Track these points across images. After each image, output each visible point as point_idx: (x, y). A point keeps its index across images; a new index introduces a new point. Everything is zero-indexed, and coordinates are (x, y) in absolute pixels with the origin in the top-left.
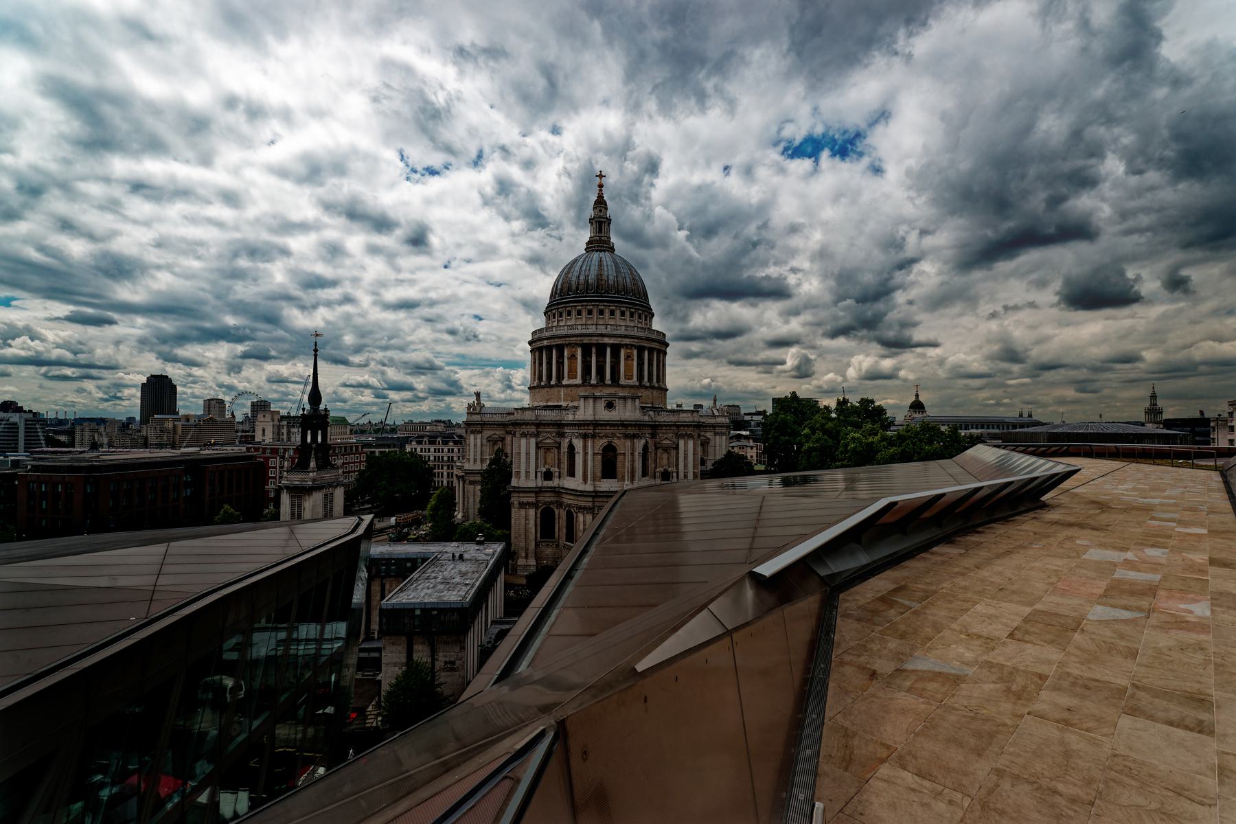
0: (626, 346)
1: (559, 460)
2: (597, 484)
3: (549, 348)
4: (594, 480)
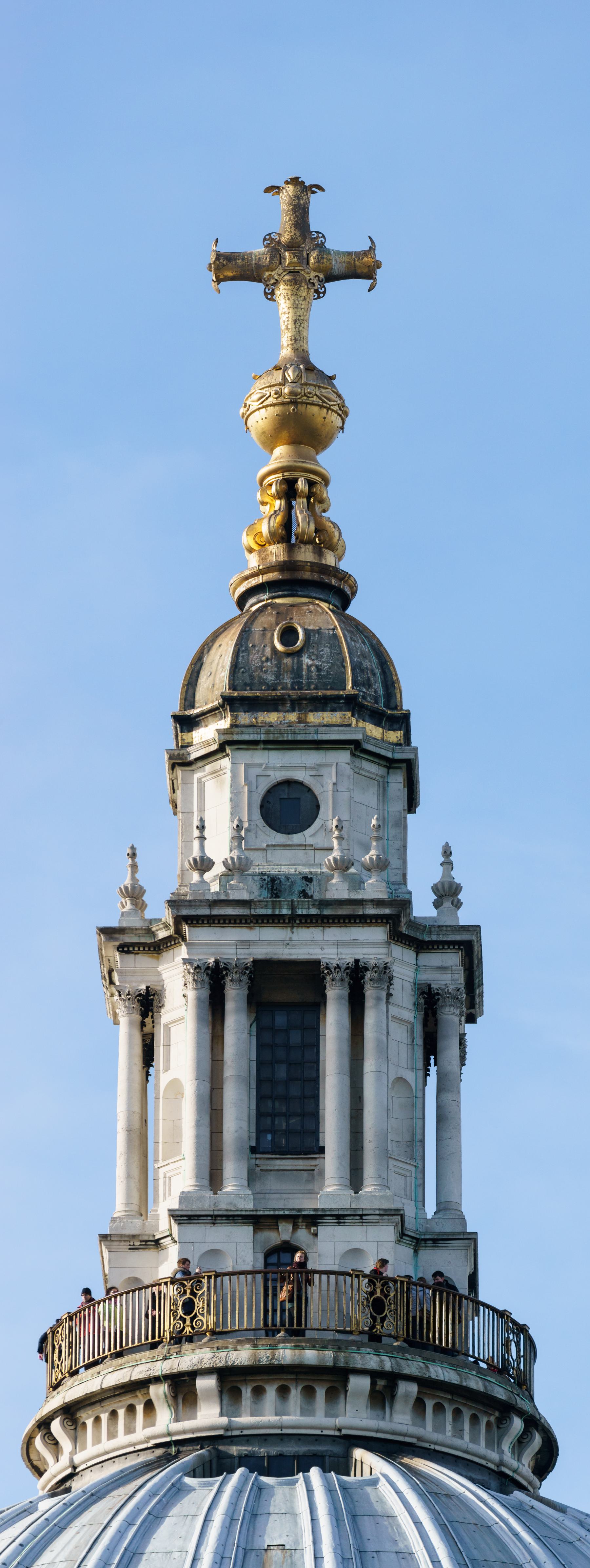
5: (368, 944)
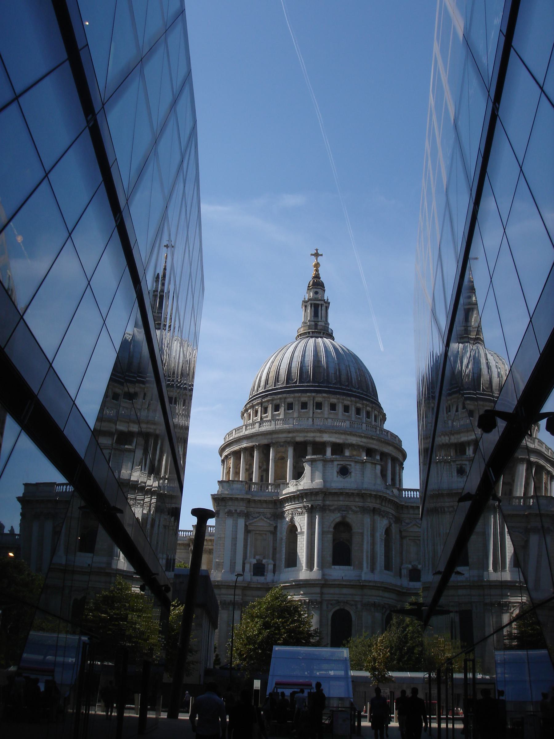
0: (351, 446)
1: (275, 549)
2: (327, 571)
3: (250, 451)
4: (322, 566)
5: (322, 302)
